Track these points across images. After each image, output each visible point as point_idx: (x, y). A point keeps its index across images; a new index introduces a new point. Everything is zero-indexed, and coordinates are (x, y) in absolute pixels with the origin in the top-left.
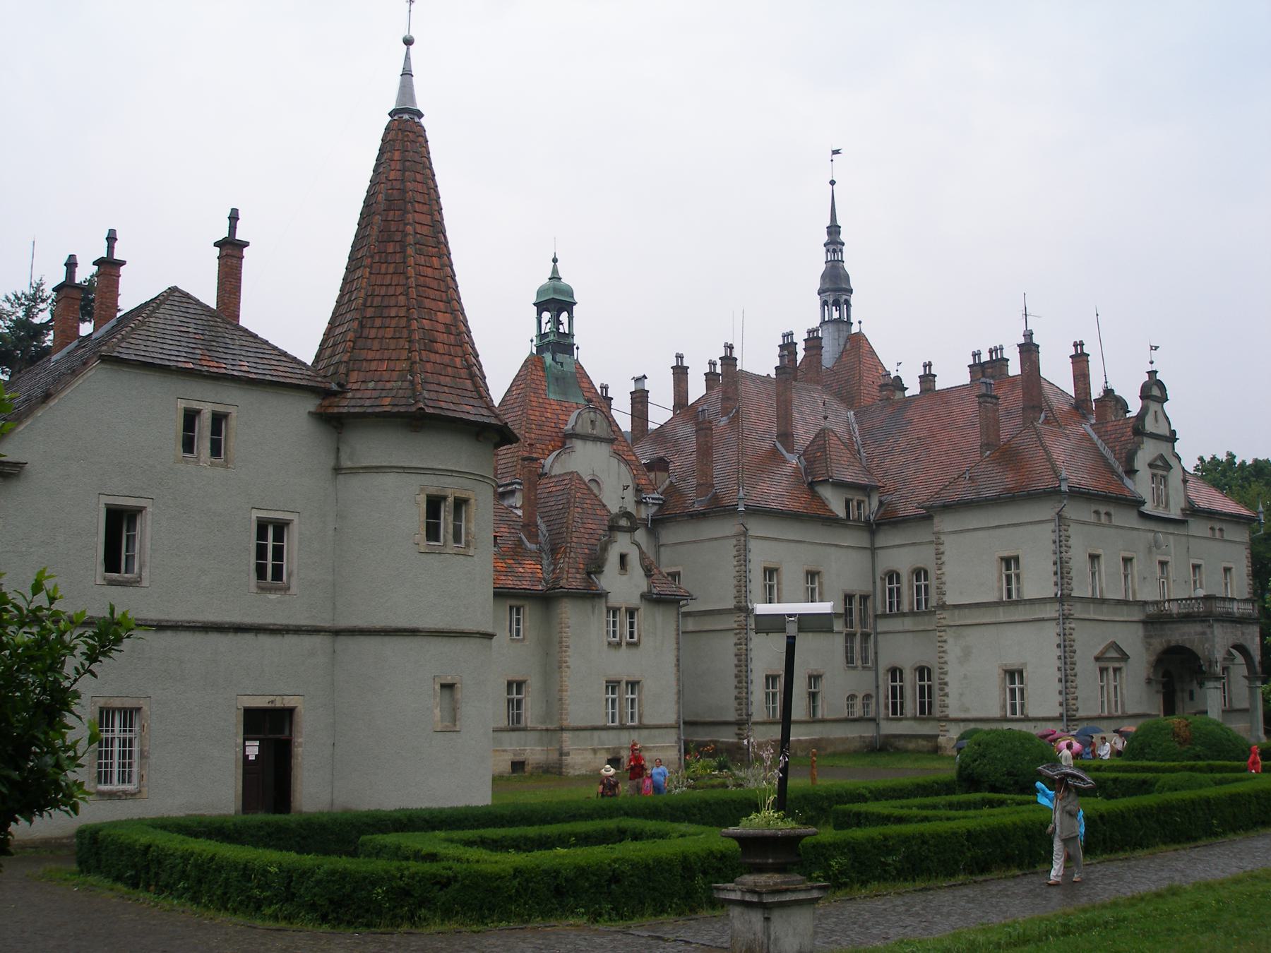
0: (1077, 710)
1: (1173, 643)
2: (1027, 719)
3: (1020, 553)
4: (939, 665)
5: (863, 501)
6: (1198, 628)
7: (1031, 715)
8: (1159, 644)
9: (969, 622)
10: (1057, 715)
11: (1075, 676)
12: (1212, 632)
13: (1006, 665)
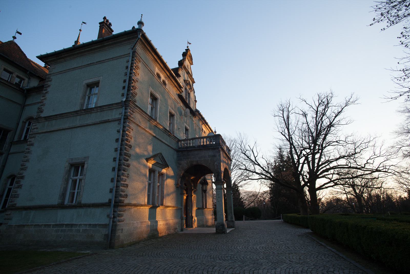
0: (126, 196)
1: (195, 163)
2: (80, 206)
3: (101, 78)
4: (22, 163)
5: (24, 80)
6: (211, 153)
7: (85, 200)
8: (185, 164)
9: (52, 129)
10: (107, 201)
11: (128, 166)
12: (220, 155)
13: (72, 159)
